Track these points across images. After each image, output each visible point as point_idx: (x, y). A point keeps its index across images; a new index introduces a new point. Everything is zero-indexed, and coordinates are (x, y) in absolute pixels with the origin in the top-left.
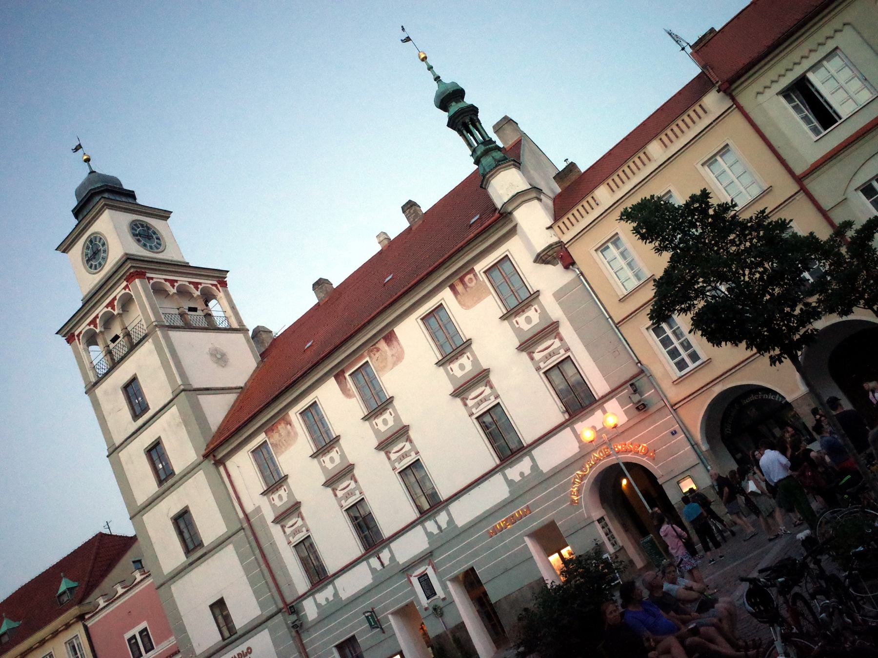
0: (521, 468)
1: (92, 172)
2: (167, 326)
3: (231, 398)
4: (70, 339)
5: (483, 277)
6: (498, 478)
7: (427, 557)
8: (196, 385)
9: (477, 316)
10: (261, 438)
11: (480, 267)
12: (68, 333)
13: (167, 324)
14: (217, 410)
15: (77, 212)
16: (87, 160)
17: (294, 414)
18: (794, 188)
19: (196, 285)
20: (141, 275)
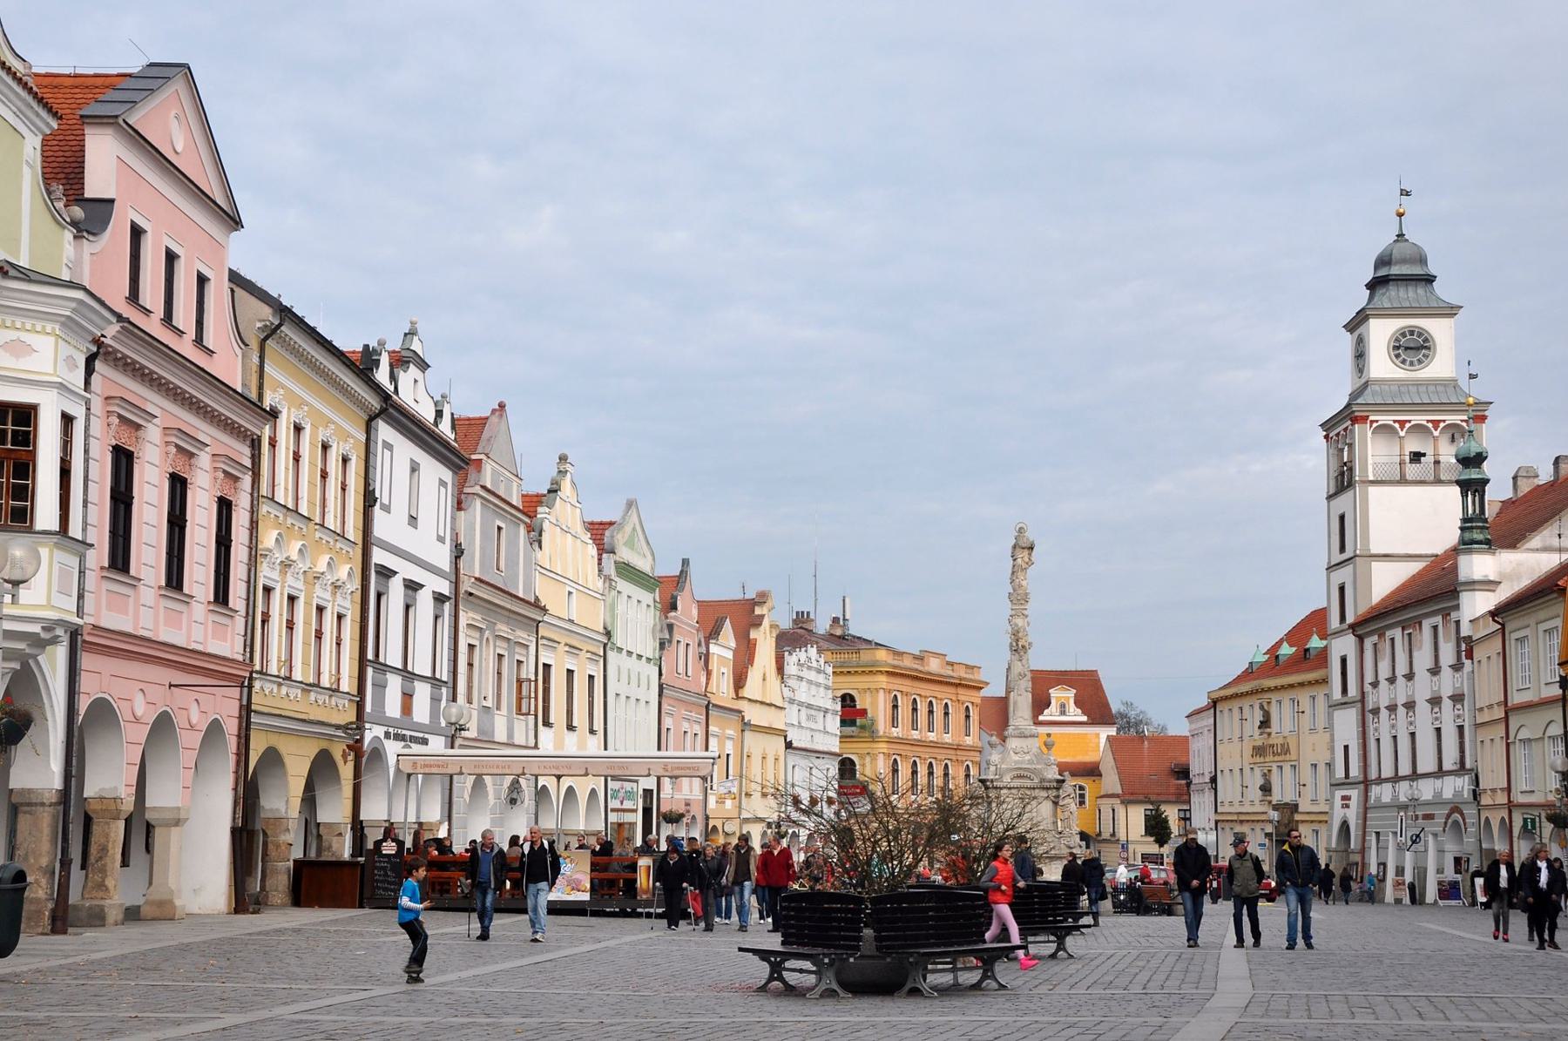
0: (1438, 782)
1: (1401, 235)
2: (1372, 482)
3: (1415, 567)
4: (1326, 437)
5: (1453, 626)
6: (1431, 780)
7: (1405, 807)
8: (1374, 551)
9: (1448, 654)
10: (1375, 638)
11: (1454, 615)
12: (1328, 426)
13: (1371, 478)
14: (1385, 581)
15: (1373, 286)
16: (1400, 215)
17: (1389, 634)
18: (1499, 713)
19: (1436, 423)
20: (1364, 419)
